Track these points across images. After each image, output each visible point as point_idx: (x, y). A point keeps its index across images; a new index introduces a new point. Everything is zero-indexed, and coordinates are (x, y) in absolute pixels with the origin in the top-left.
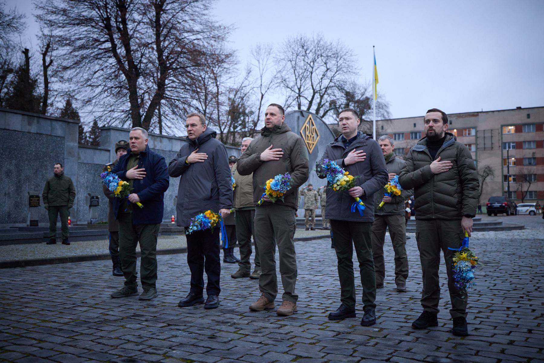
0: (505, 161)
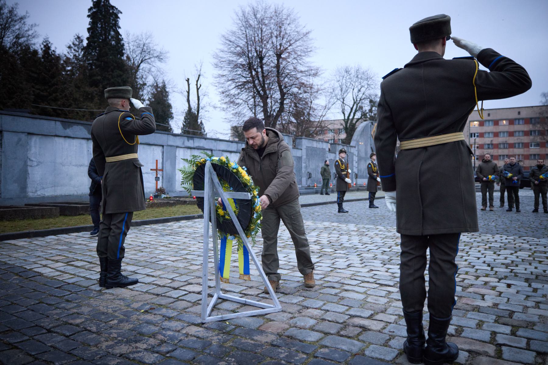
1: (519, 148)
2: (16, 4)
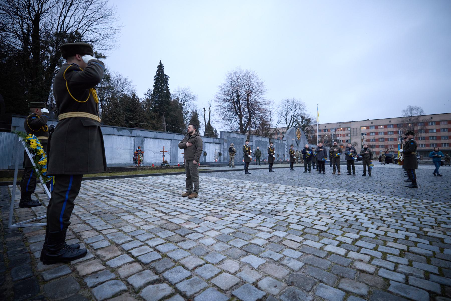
0: (362, 140)
1: (391, 141)
2: (128, 77)
